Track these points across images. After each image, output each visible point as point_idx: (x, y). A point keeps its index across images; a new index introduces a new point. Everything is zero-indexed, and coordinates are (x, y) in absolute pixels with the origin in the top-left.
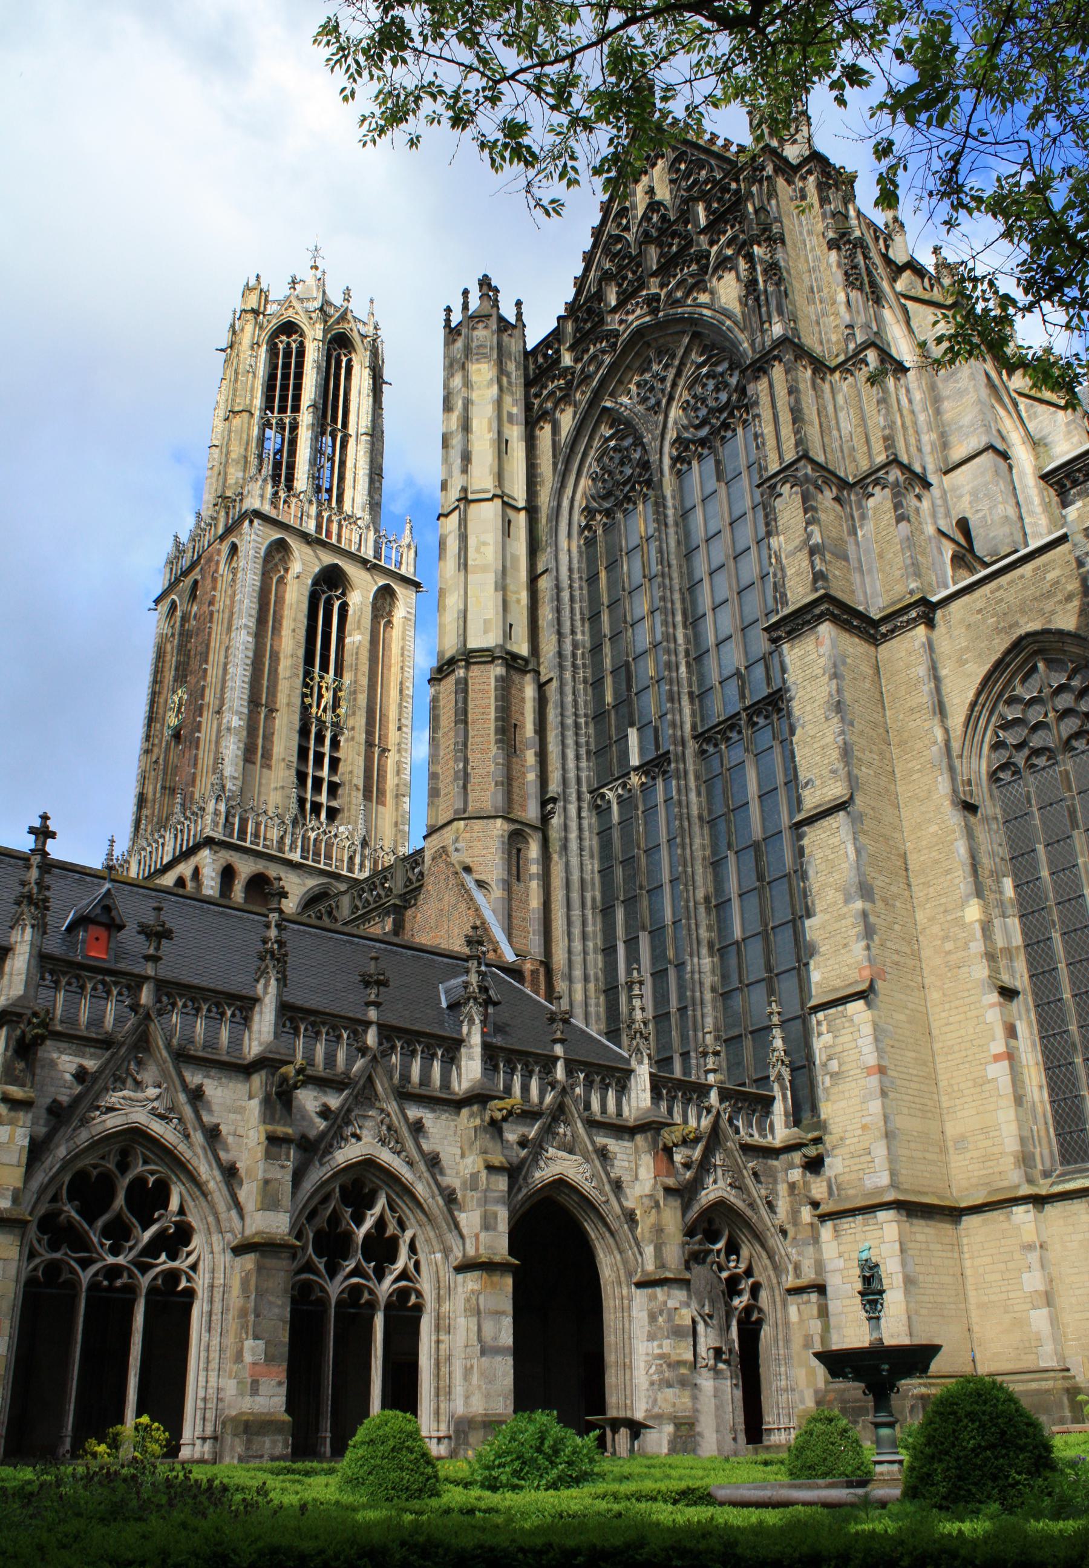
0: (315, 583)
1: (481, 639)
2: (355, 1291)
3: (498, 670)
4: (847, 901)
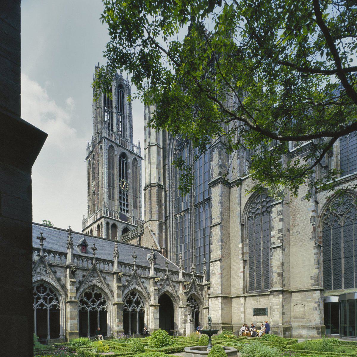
1: (154, 181)
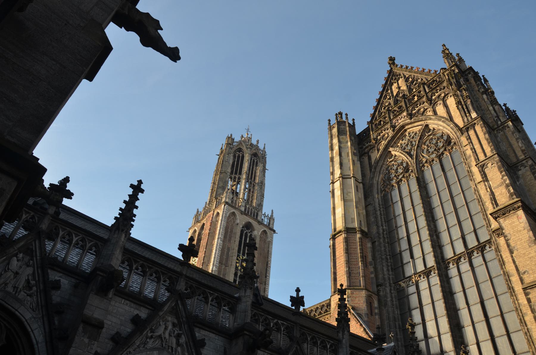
0: (243, 227)
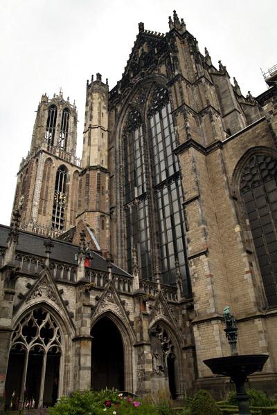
2: (37, 347)
3: (99, 172)
4: (199, 226)
